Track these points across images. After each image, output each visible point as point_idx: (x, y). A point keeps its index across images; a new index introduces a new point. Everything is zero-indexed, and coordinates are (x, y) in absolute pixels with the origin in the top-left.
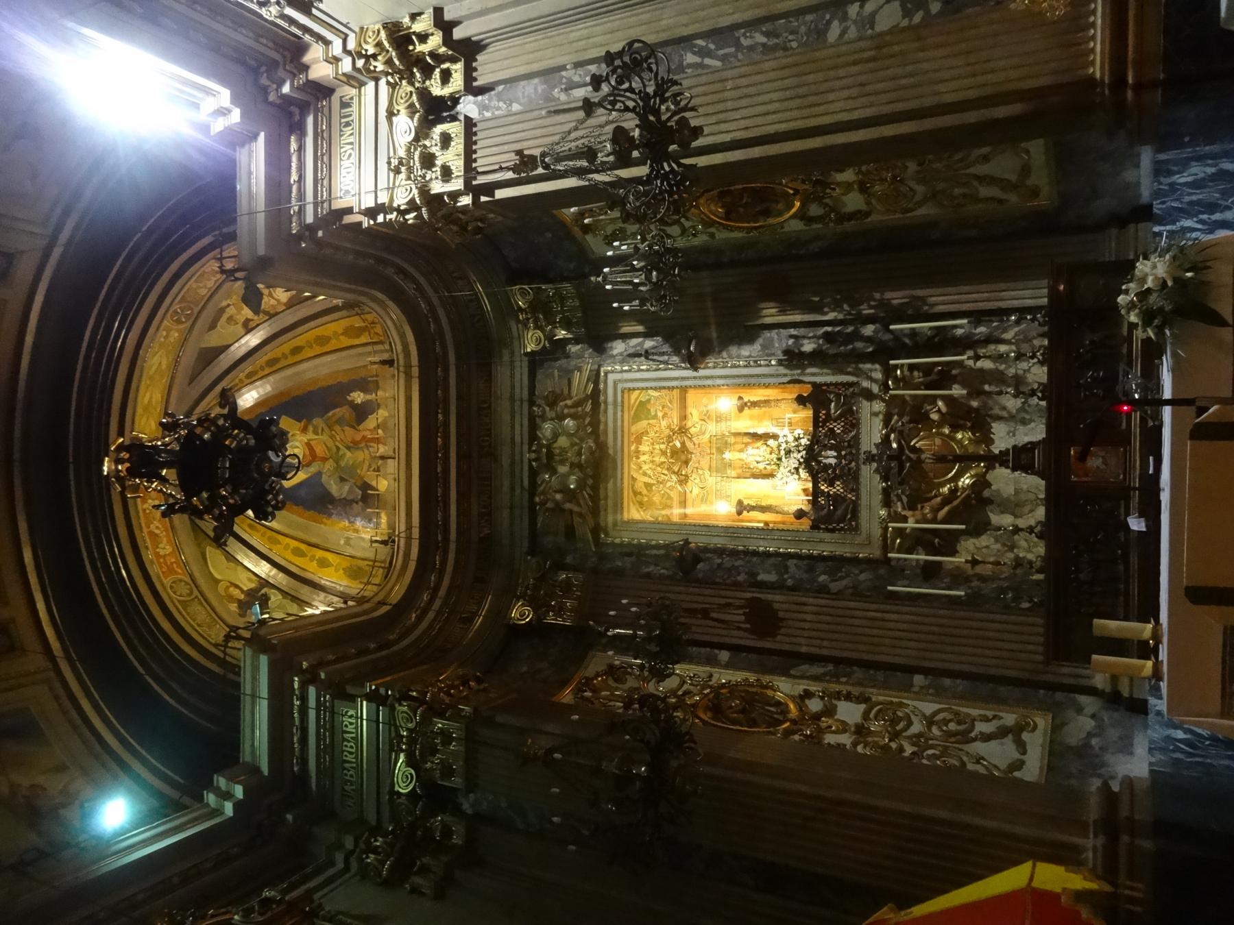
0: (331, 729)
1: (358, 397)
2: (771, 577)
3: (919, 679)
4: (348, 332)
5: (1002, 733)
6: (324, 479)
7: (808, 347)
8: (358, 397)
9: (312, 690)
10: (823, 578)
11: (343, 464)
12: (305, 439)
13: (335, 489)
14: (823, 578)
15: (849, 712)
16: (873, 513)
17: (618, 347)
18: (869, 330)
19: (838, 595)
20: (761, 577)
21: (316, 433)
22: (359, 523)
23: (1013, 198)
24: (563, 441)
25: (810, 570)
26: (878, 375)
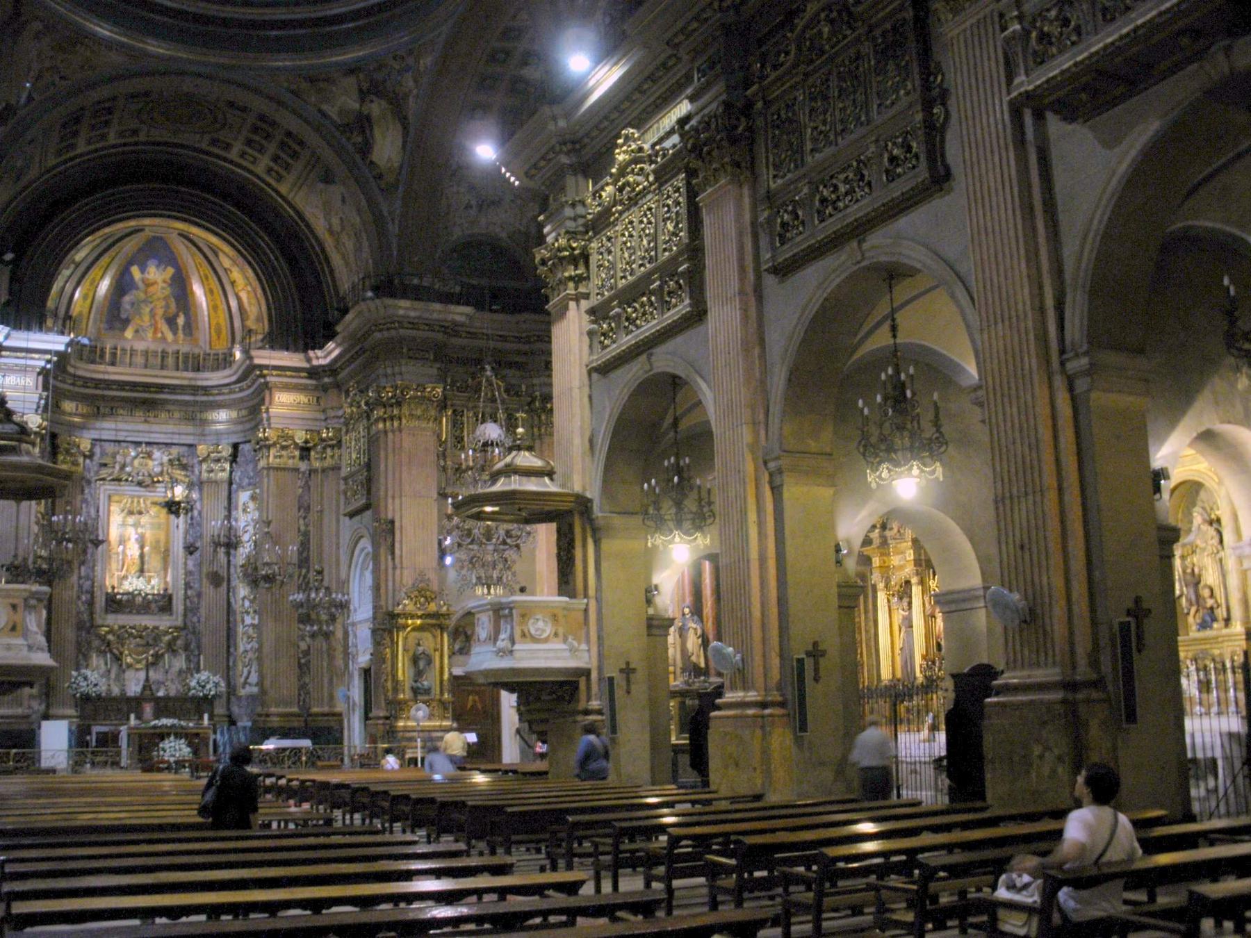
1: (181, 321)
2: (83, 573)
4: (218, 324)
6: (134, 292)
8: (181, 321)
9: (42, 363)
10: (84, 598)
11: (142, 305)
12: (159, 280)
13: (127, 299)
14: (84, 598)
20: (83, 569)
21: (163, 288)
23: (242, 680)
25: (87, 592)
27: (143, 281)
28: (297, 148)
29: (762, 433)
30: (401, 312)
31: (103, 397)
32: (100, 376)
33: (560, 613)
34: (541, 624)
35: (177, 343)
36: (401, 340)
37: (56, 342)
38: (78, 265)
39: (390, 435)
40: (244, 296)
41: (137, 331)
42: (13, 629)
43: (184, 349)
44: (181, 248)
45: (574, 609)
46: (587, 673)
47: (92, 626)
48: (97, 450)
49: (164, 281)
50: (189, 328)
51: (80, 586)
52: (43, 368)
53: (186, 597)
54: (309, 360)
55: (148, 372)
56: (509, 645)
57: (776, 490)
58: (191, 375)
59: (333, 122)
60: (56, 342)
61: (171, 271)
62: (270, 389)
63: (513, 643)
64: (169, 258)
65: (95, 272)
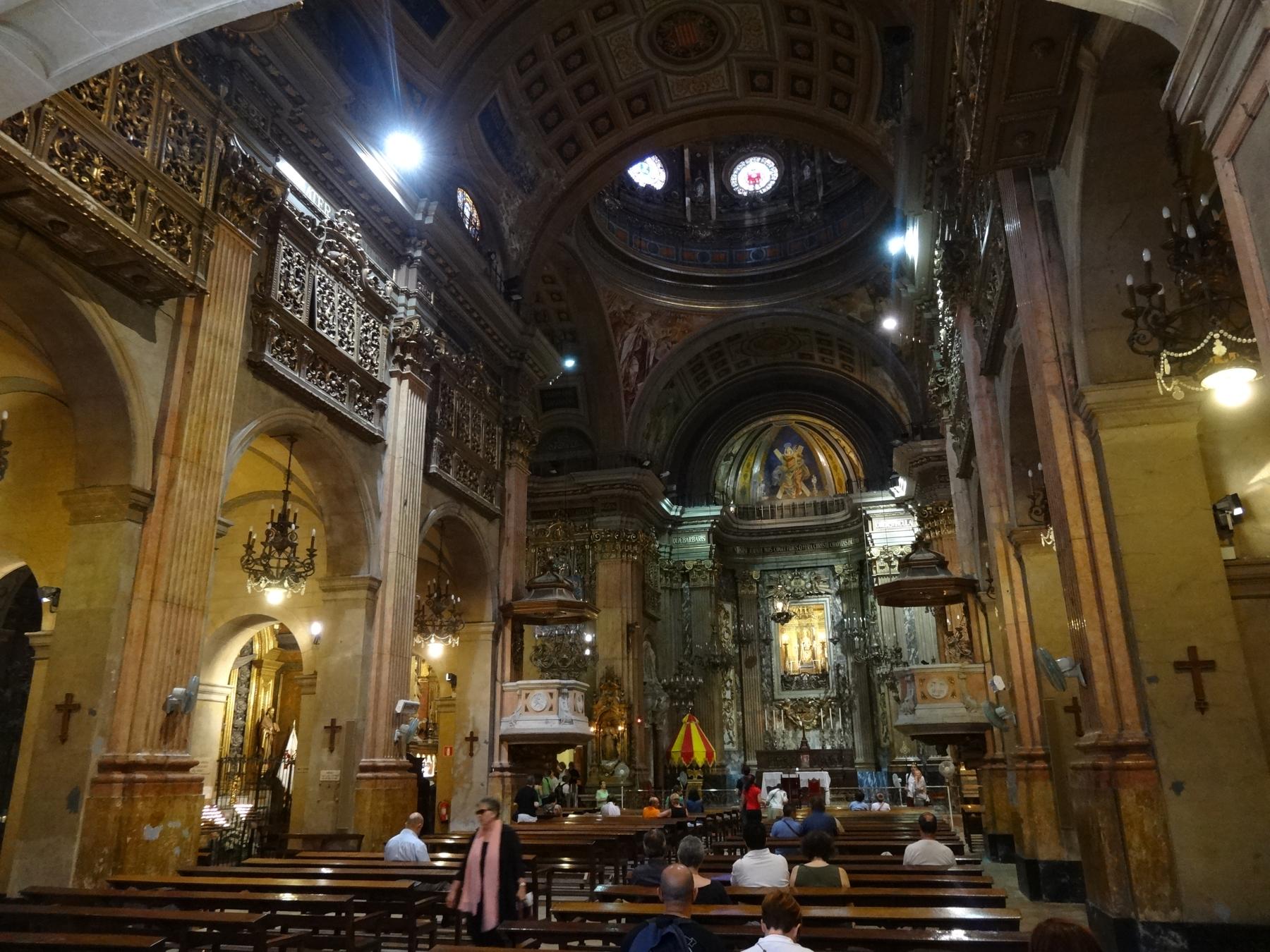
0: (698, 532)
1: (814, 481)
3: (740, 713)
5: (731, 738)
7: (841, 672)
8: (814, 481)
9: (709, 525)
12: (795, 456)
13: (775, 472)
15: (728, 695)
16: (788, 696)
17: (838, 601)
18: (847, 691)
19: (761, 686)
22: (763, 485)
24: (803, 582)
26: (832, 695)
27: (784, 458)
28: (849, 346)
29: (1005, 512)
30: (925, 450)
31: (764, 542)
32: (759, 527)
33: (955, 676)
34: (938, 687)
35: (809, 496)
36: (934, 468)
37: (715, 511)
38: (735, 457)
39: (935, 543)
40: (852, 455)
41: (785, 493)
42: (551, 709)
43: (819, 500)
44: (805, 433)
45: (973, 673)
46: (988, 726)
47: (774, 700)
48: (766, 577)
49: (798, 456)
50: (821, 484)
51: (762, 672)
52: (711, 529)
53: (838, 675)
54: (893, 495)
55: (794, 519)
56: (912, 706)
57: (1020, 560)
58: (822, 517)
59: (859, 323)
60: (715, 511)
61: (801, 448)
62: (871, 519)
63: (916, 705)
64: (798, 440)
65: (749, 458)
